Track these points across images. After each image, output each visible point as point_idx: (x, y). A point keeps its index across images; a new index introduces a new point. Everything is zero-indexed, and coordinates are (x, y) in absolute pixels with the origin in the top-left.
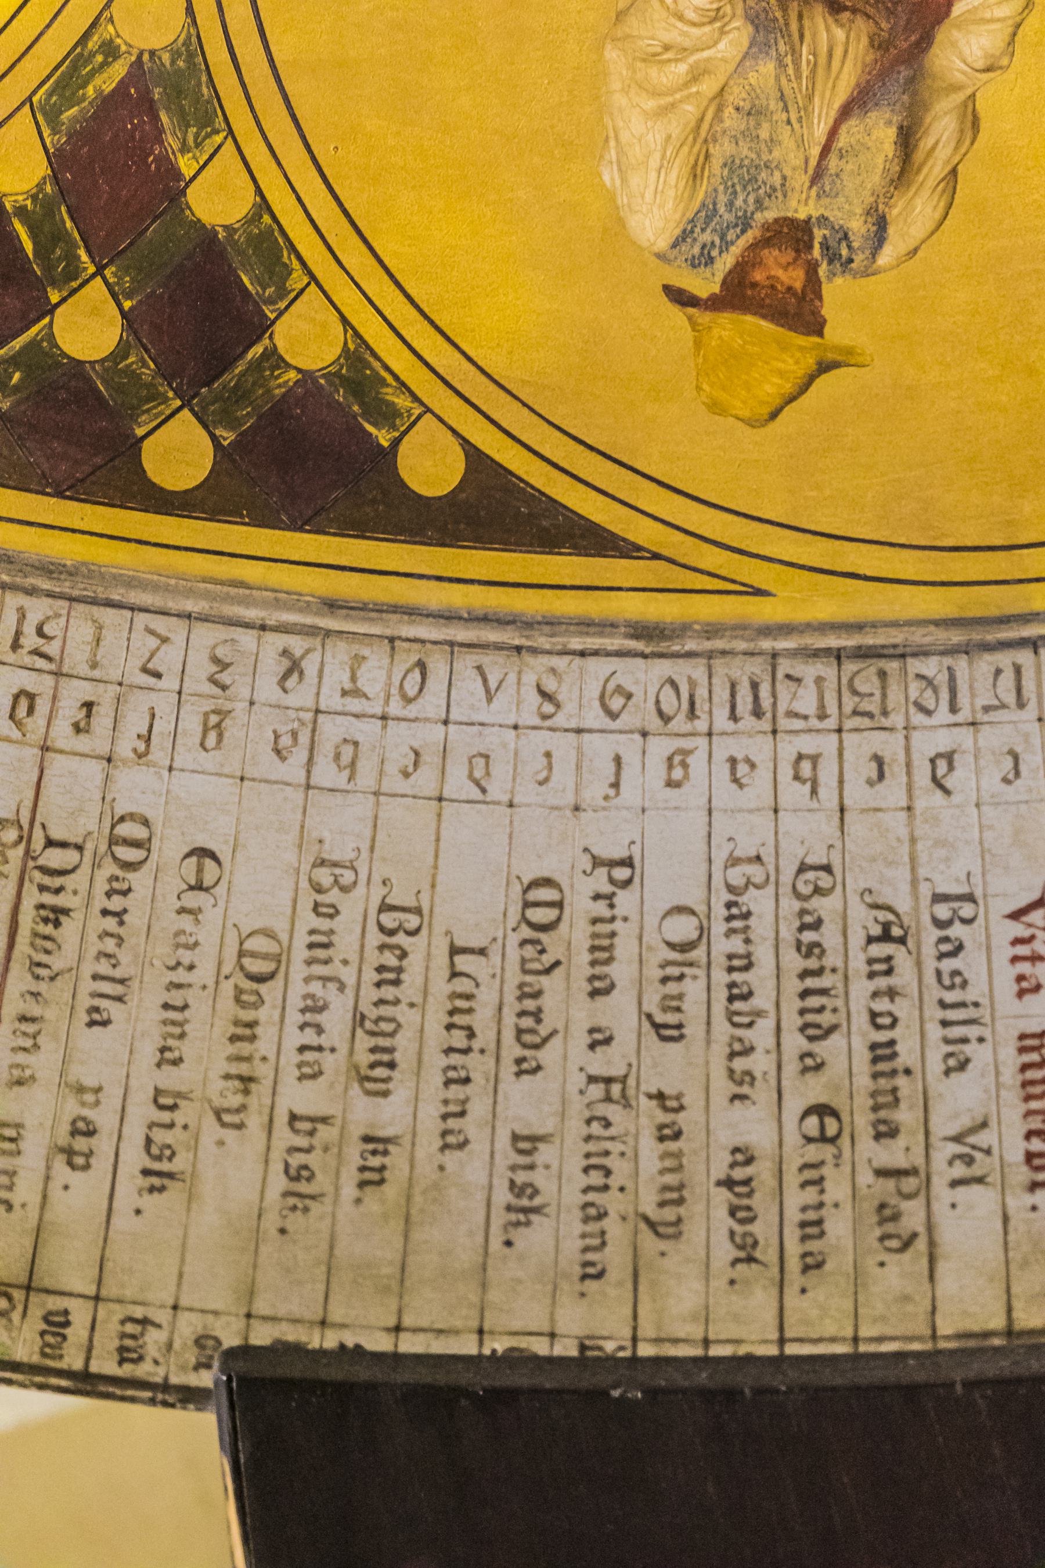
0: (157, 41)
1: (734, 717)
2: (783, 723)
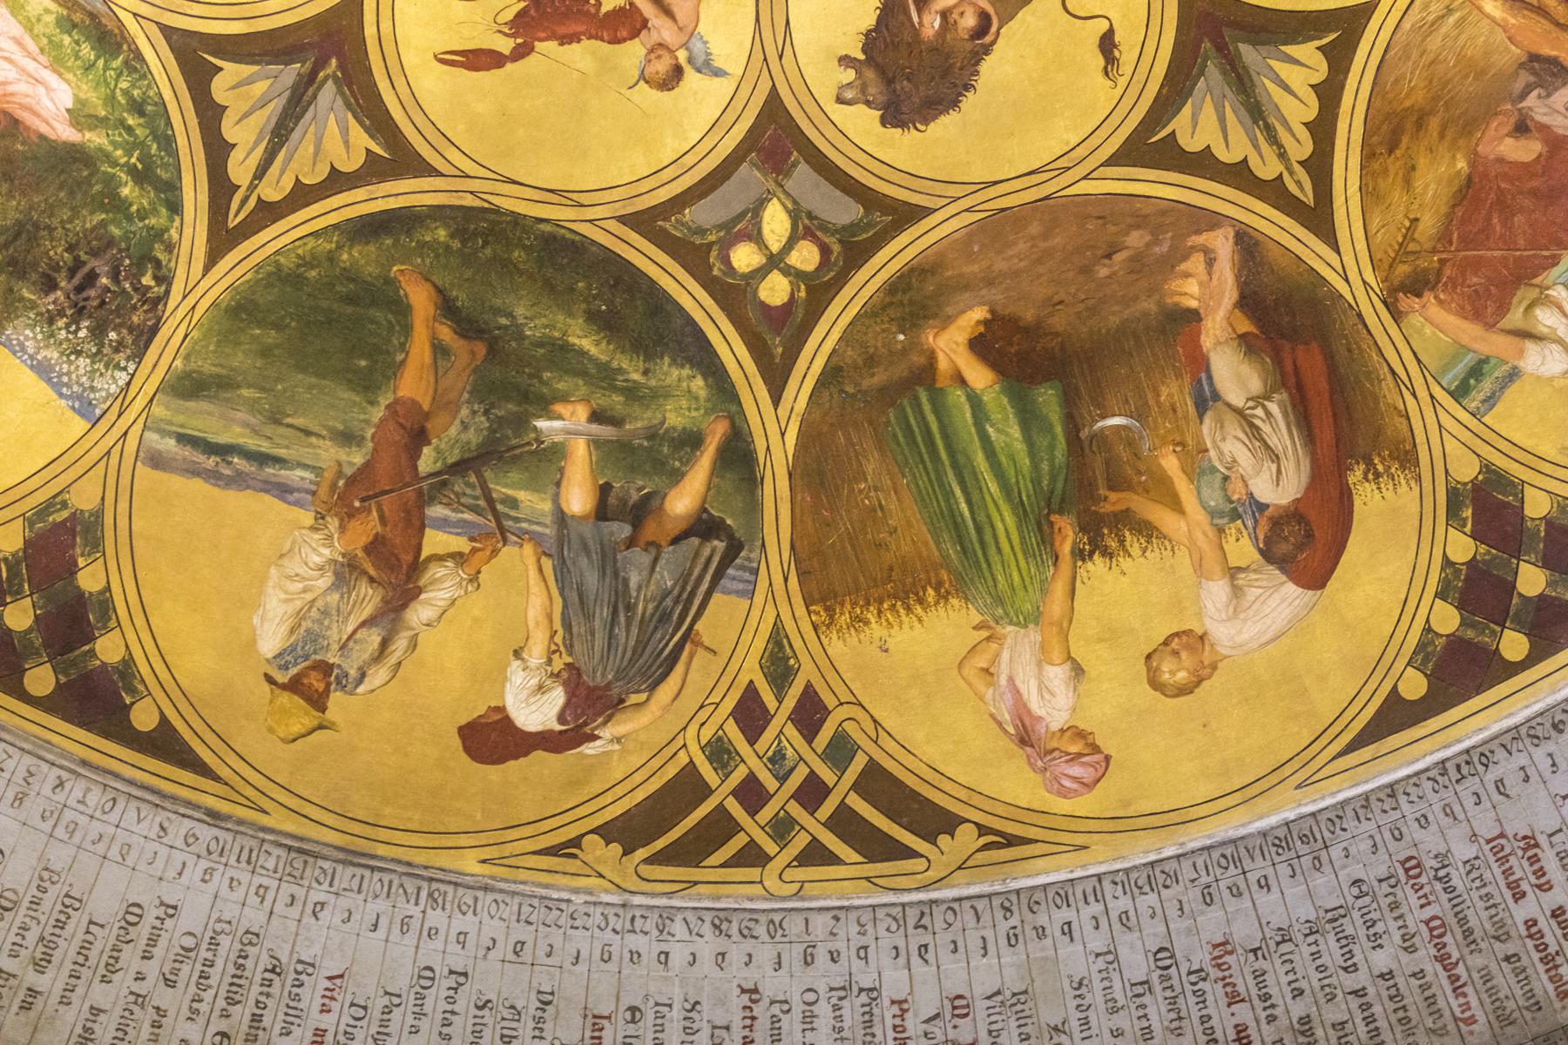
1: (238, 861)
2: (258, 870)
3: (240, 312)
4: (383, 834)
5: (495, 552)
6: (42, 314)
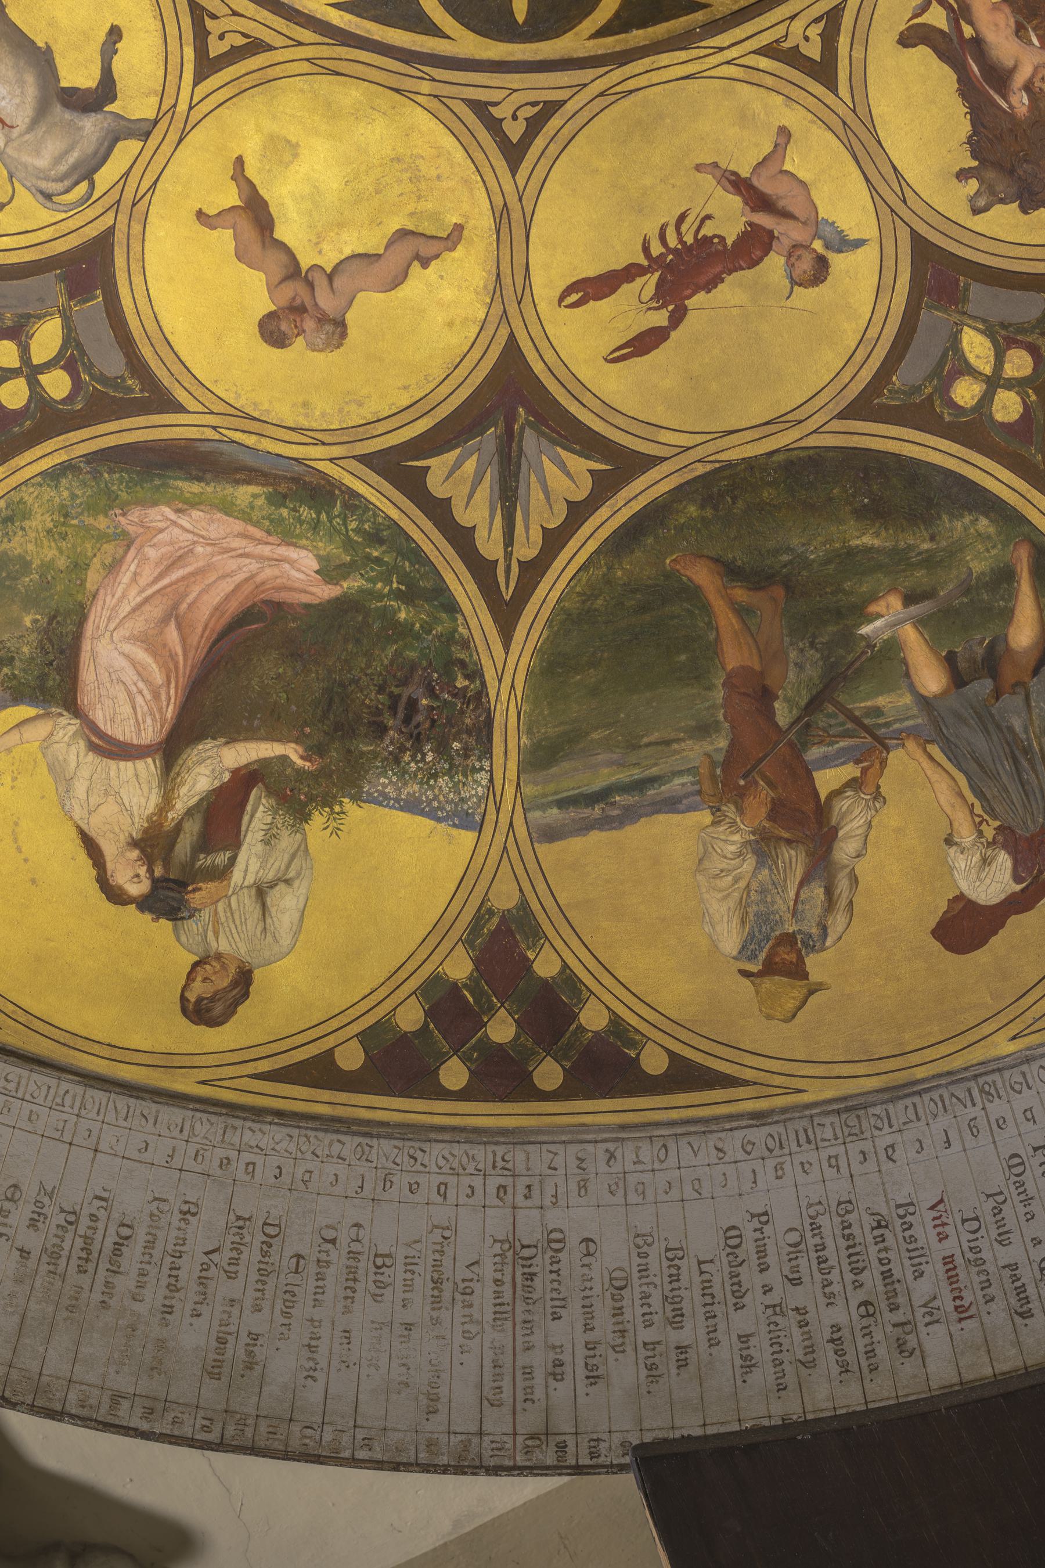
1: (799, 1145)
2: (821, 1144)
3: (553, 669)
4: (915, 1059)
5: (883, 763)
6: (386, 759)
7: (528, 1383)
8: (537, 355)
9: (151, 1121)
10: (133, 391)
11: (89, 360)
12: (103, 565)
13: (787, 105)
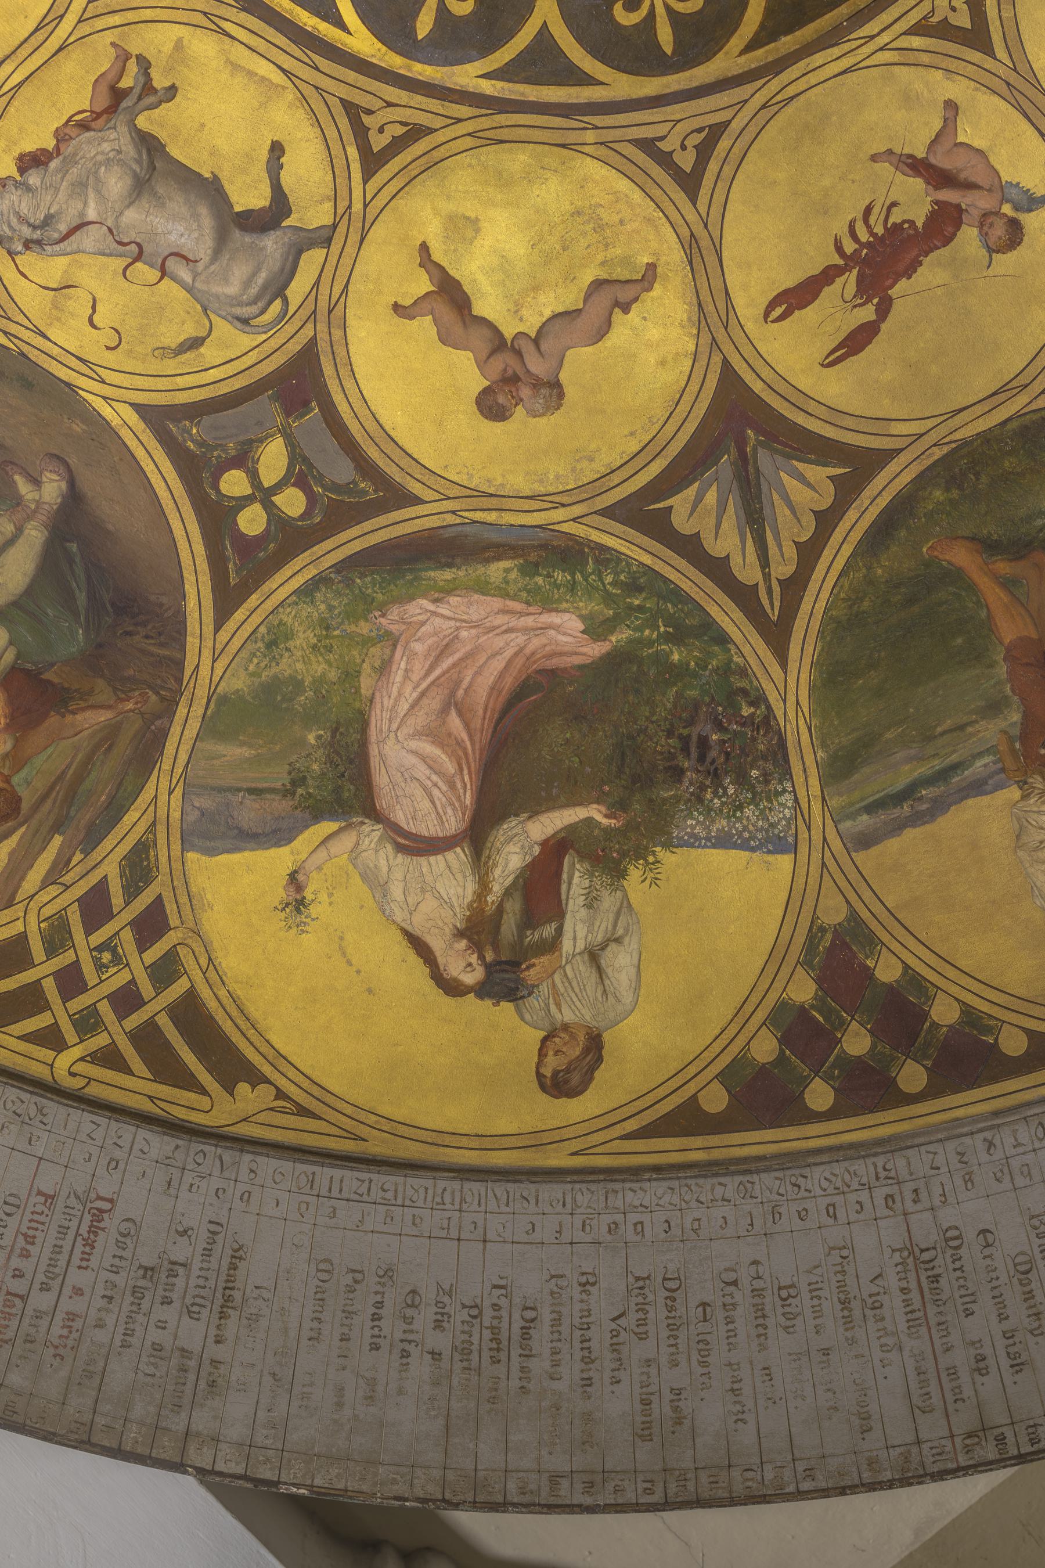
0: (841, 918)
3: (834, 679)
6: (689, 800)
7: (954, 1384)
8: (754, 375)
9: (533, 1202)
10: (367, 493)
11: (318, 472)
12: (374, 668)
13: (947, 79)
